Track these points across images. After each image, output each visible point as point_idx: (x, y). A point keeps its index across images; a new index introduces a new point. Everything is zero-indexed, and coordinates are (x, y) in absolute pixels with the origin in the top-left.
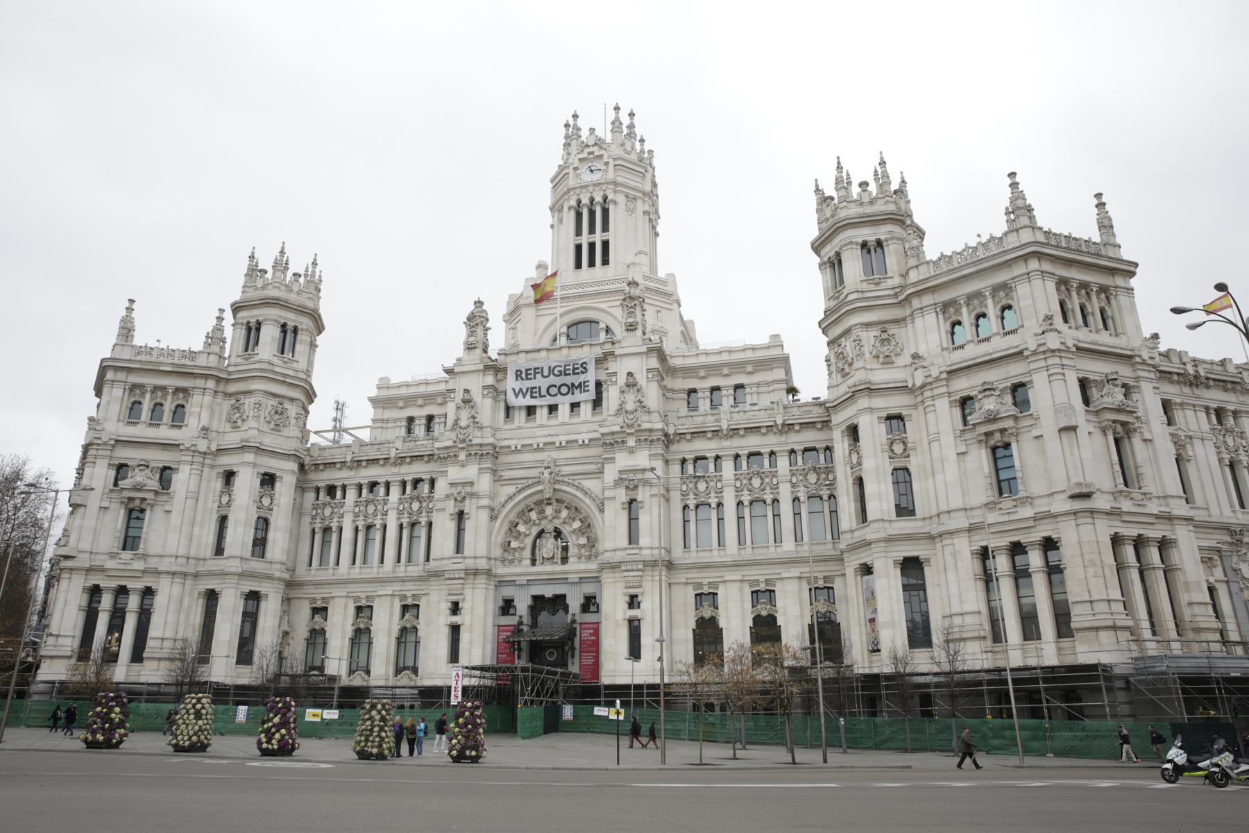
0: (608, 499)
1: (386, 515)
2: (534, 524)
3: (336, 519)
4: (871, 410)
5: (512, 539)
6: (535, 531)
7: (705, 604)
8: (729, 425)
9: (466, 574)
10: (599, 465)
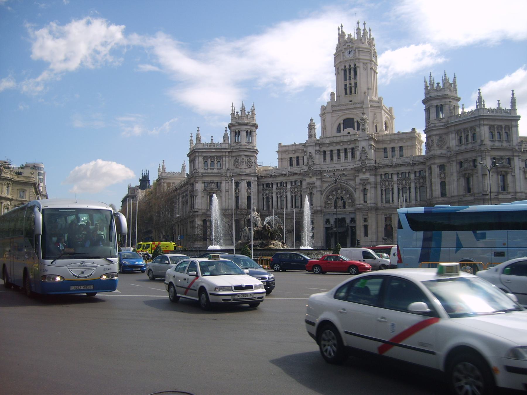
0: (357, 188)
1: (287, 193)
3: (270, 194)
4: (434, 164)
5: (327, 200)
6: (335, 197)
7: (388, 220)
8: (395, 164)
9: (314, 212)
10: (354, 177)
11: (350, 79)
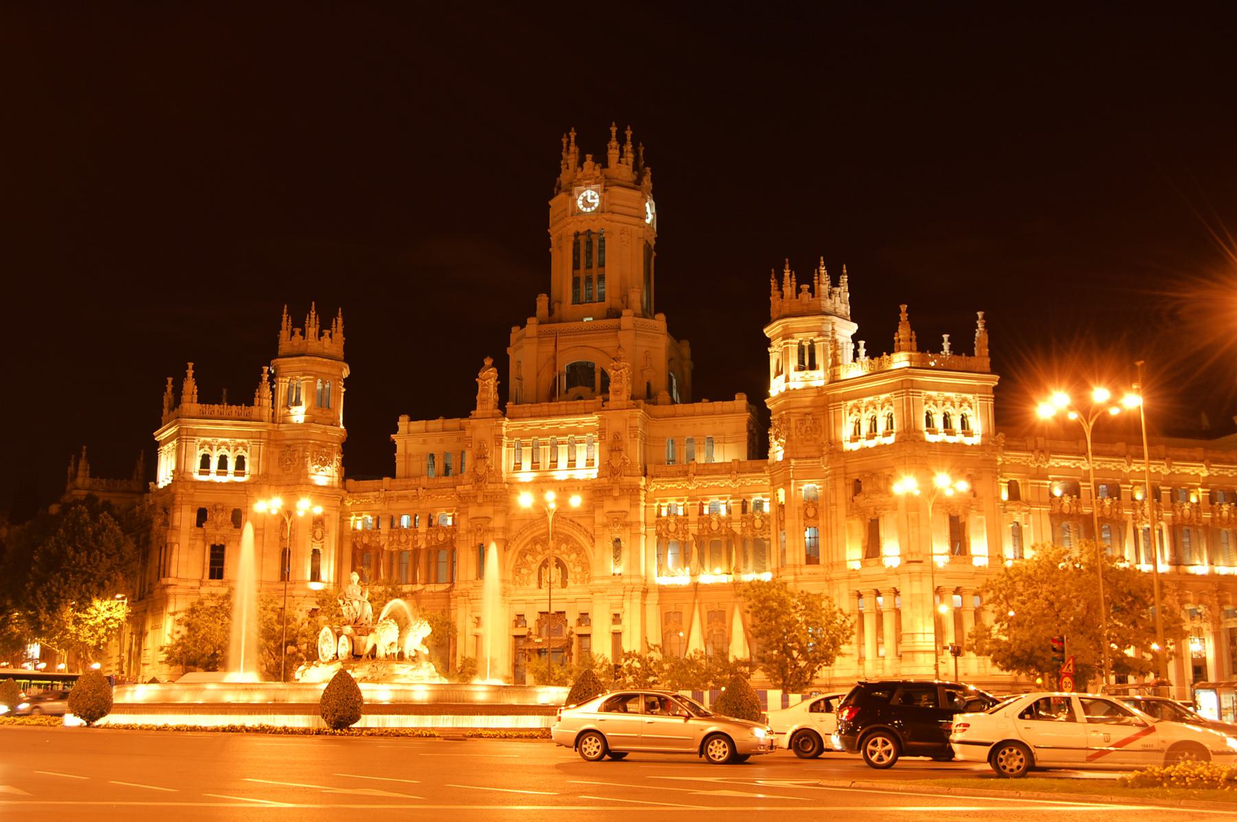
2: (540, 553)
6: (540, 558)
11: (589, 267)
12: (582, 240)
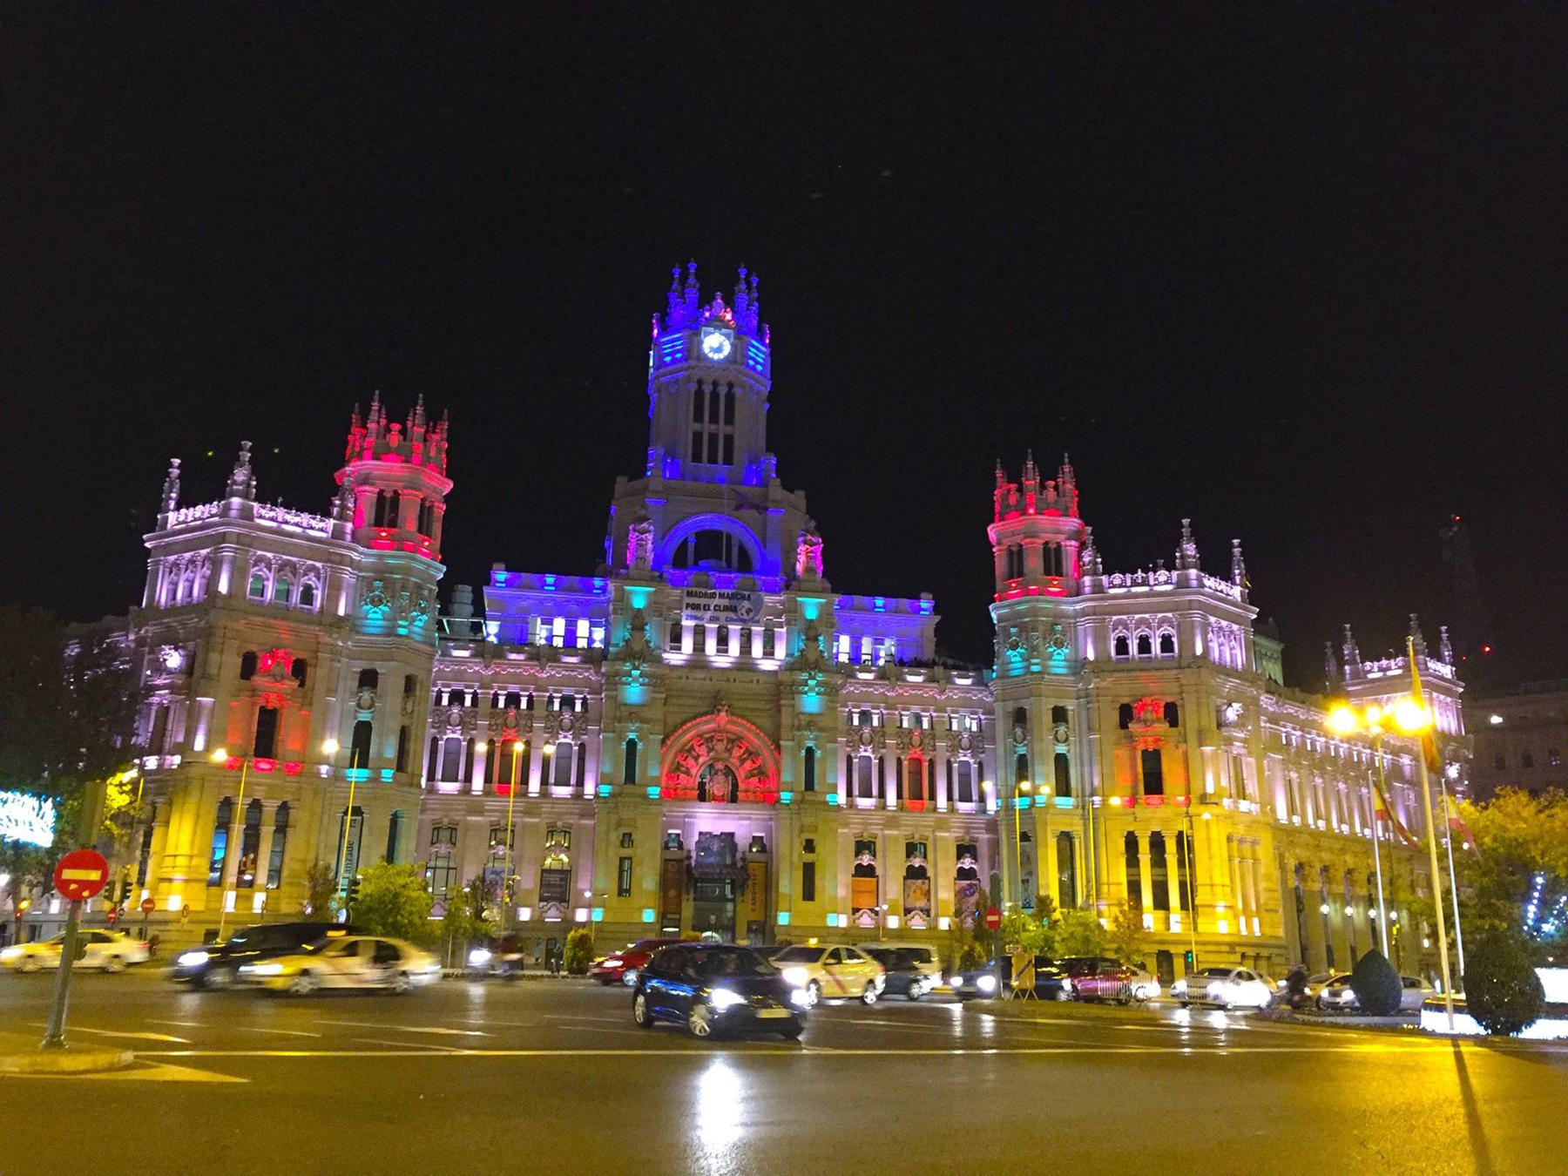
12: (707, 389)
